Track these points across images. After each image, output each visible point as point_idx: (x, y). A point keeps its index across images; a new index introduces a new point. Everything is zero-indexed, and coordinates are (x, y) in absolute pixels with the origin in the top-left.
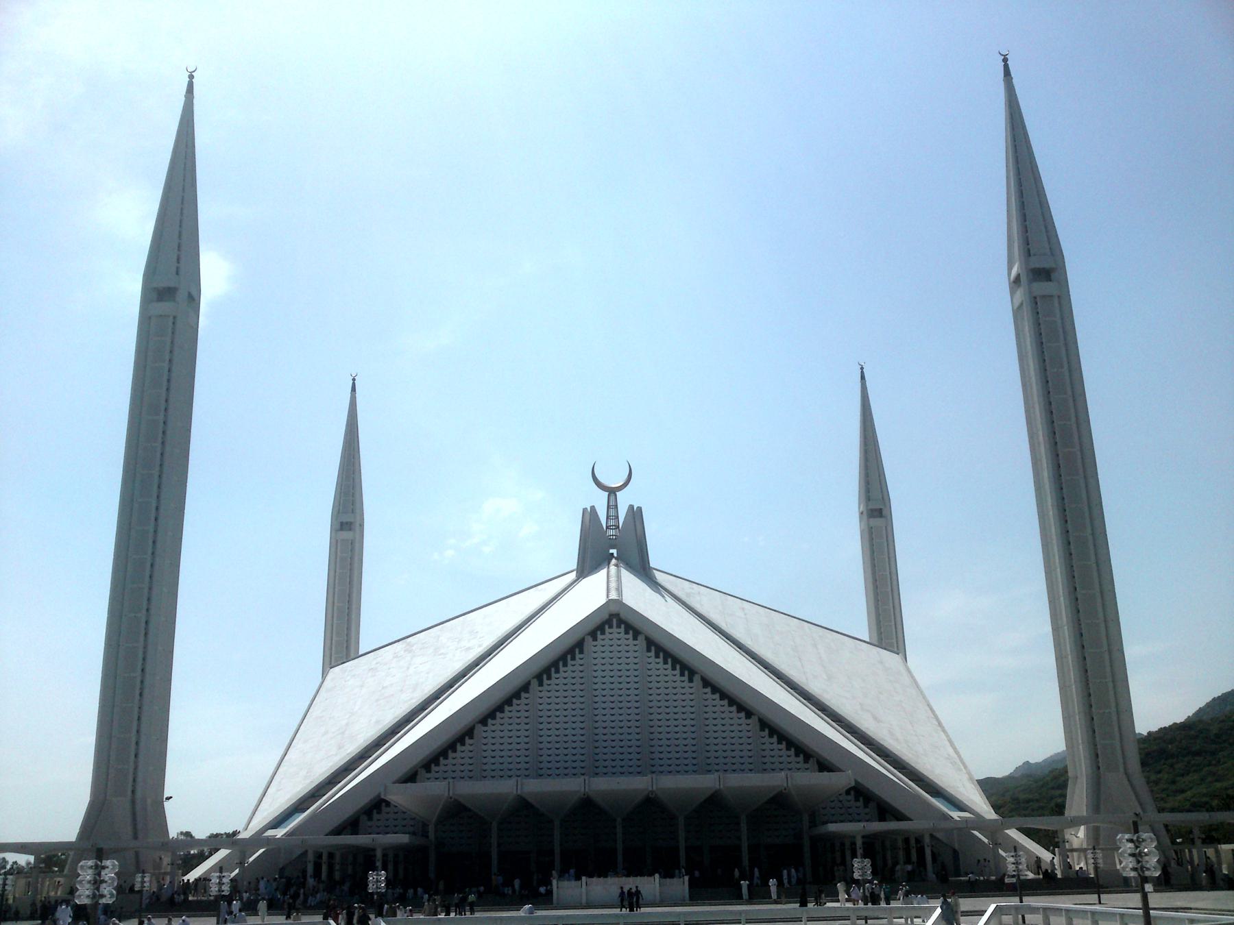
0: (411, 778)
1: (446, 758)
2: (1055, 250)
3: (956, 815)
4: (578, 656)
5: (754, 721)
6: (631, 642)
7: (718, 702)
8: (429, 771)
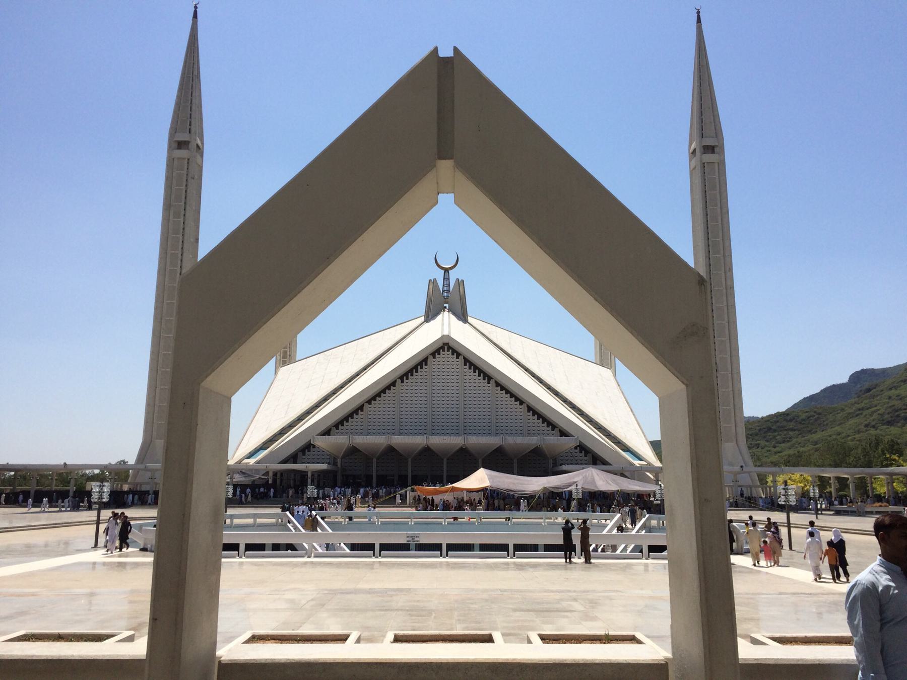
0: (327, 432)
1: (347, 421)
2: (718, 133)
3: (637, 463)
4: (424, 366)
5: (524, 406)
6: (455, 359)
7: (504, 395)
8: (337, 428)
